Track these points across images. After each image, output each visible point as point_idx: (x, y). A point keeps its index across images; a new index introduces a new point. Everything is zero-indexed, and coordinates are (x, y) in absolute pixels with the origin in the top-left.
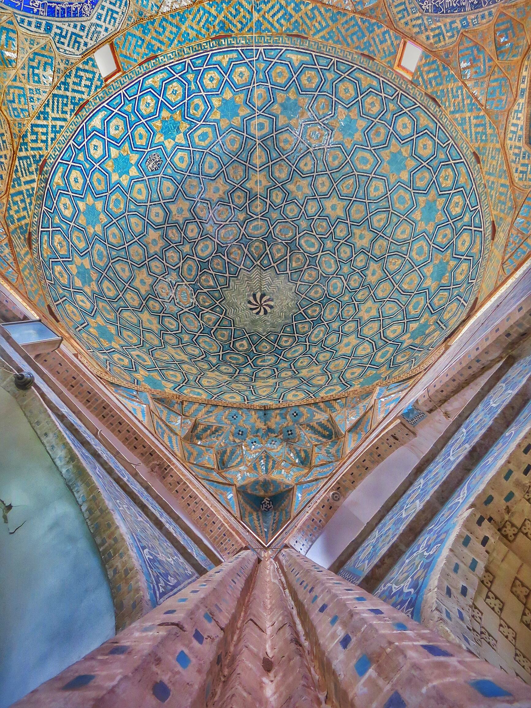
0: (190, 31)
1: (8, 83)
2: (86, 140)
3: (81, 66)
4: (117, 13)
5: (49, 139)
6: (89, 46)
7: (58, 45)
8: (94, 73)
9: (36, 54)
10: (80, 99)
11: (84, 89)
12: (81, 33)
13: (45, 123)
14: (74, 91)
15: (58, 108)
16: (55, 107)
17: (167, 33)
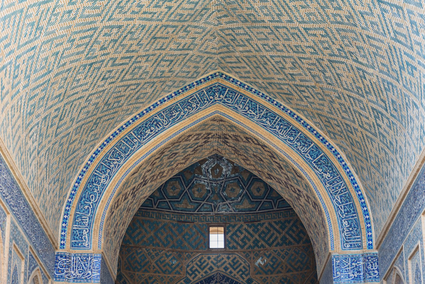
0: (148, 229)
1: (296, 273)
2: (263, 200)
3: (239, 248)
4: (197, 264)
5: (291, 224)
6: (226, 256)
7: (248, 268)
8: (231, 237)
9: (266, 273)
10: (250, 227)
11: (244, 232)
12: (228, 266)
13: (288, 236)
14: (252, 236)
15: (271, 237)
16: (273, 238)
17: (165, 235)
